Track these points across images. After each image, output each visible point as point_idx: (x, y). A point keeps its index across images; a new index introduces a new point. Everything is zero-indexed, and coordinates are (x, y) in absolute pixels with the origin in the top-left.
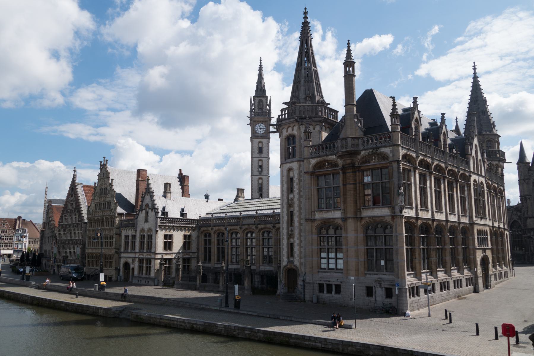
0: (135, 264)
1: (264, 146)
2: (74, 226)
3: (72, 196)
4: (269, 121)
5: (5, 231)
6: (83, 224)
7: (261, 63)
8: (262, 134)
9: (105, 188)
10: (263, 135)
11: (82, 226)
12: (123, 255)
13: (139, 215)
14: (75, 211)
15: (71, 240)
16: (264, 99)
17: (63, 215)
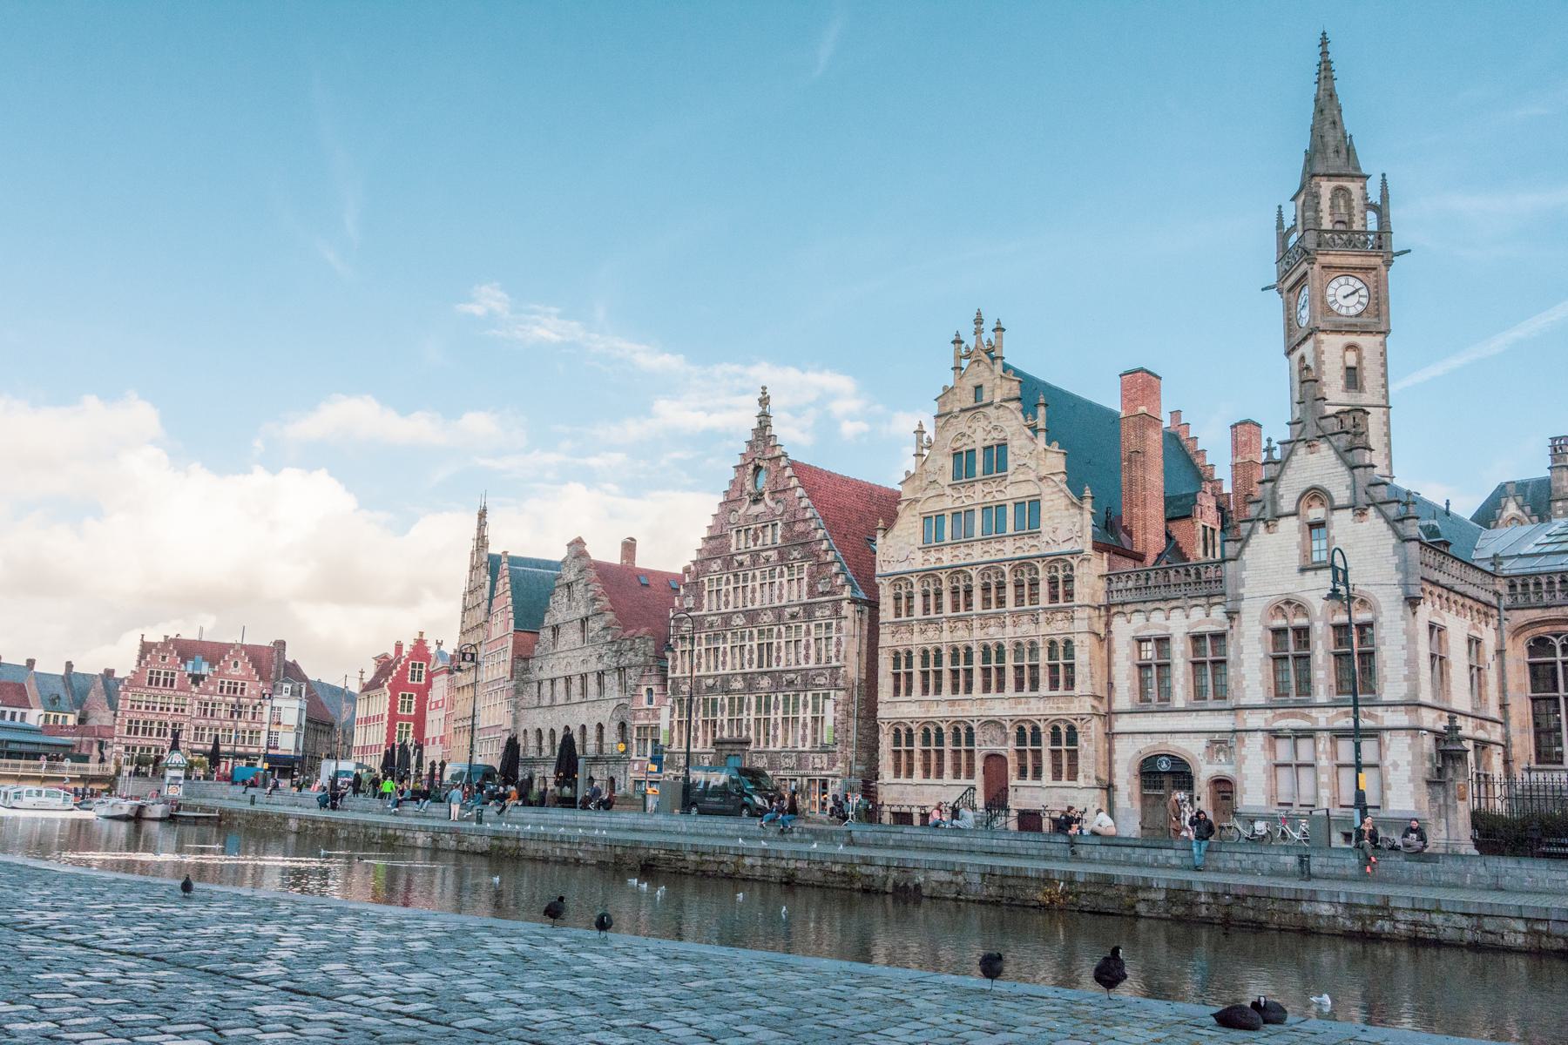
0: (1244, 758)
1: (1365, 363)
2: (779, 617)
3: (756, 501)
4: (1383, 268)
5: (239, 687)
6: (844, 604)
7: (1324, 53)
8: (1357, 316)
9: (987, 449)
10: (1359, 320)
11: (843, 613)
12: (1121, 724)
13: (1253, 541)
14: (782, 557)
15: (766, 673)
16: (1354, 186)
17: (706, 580)
